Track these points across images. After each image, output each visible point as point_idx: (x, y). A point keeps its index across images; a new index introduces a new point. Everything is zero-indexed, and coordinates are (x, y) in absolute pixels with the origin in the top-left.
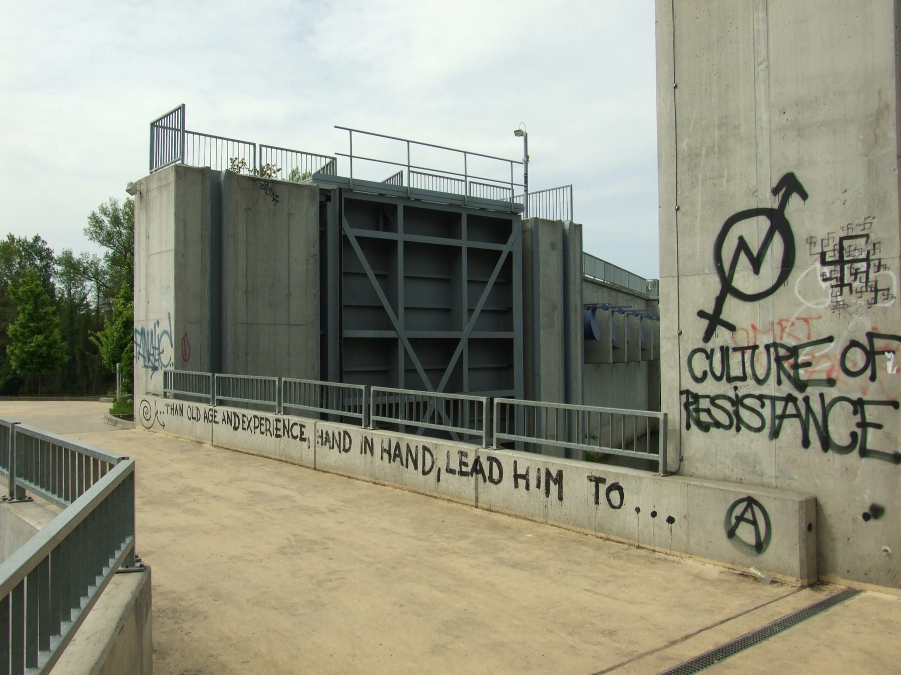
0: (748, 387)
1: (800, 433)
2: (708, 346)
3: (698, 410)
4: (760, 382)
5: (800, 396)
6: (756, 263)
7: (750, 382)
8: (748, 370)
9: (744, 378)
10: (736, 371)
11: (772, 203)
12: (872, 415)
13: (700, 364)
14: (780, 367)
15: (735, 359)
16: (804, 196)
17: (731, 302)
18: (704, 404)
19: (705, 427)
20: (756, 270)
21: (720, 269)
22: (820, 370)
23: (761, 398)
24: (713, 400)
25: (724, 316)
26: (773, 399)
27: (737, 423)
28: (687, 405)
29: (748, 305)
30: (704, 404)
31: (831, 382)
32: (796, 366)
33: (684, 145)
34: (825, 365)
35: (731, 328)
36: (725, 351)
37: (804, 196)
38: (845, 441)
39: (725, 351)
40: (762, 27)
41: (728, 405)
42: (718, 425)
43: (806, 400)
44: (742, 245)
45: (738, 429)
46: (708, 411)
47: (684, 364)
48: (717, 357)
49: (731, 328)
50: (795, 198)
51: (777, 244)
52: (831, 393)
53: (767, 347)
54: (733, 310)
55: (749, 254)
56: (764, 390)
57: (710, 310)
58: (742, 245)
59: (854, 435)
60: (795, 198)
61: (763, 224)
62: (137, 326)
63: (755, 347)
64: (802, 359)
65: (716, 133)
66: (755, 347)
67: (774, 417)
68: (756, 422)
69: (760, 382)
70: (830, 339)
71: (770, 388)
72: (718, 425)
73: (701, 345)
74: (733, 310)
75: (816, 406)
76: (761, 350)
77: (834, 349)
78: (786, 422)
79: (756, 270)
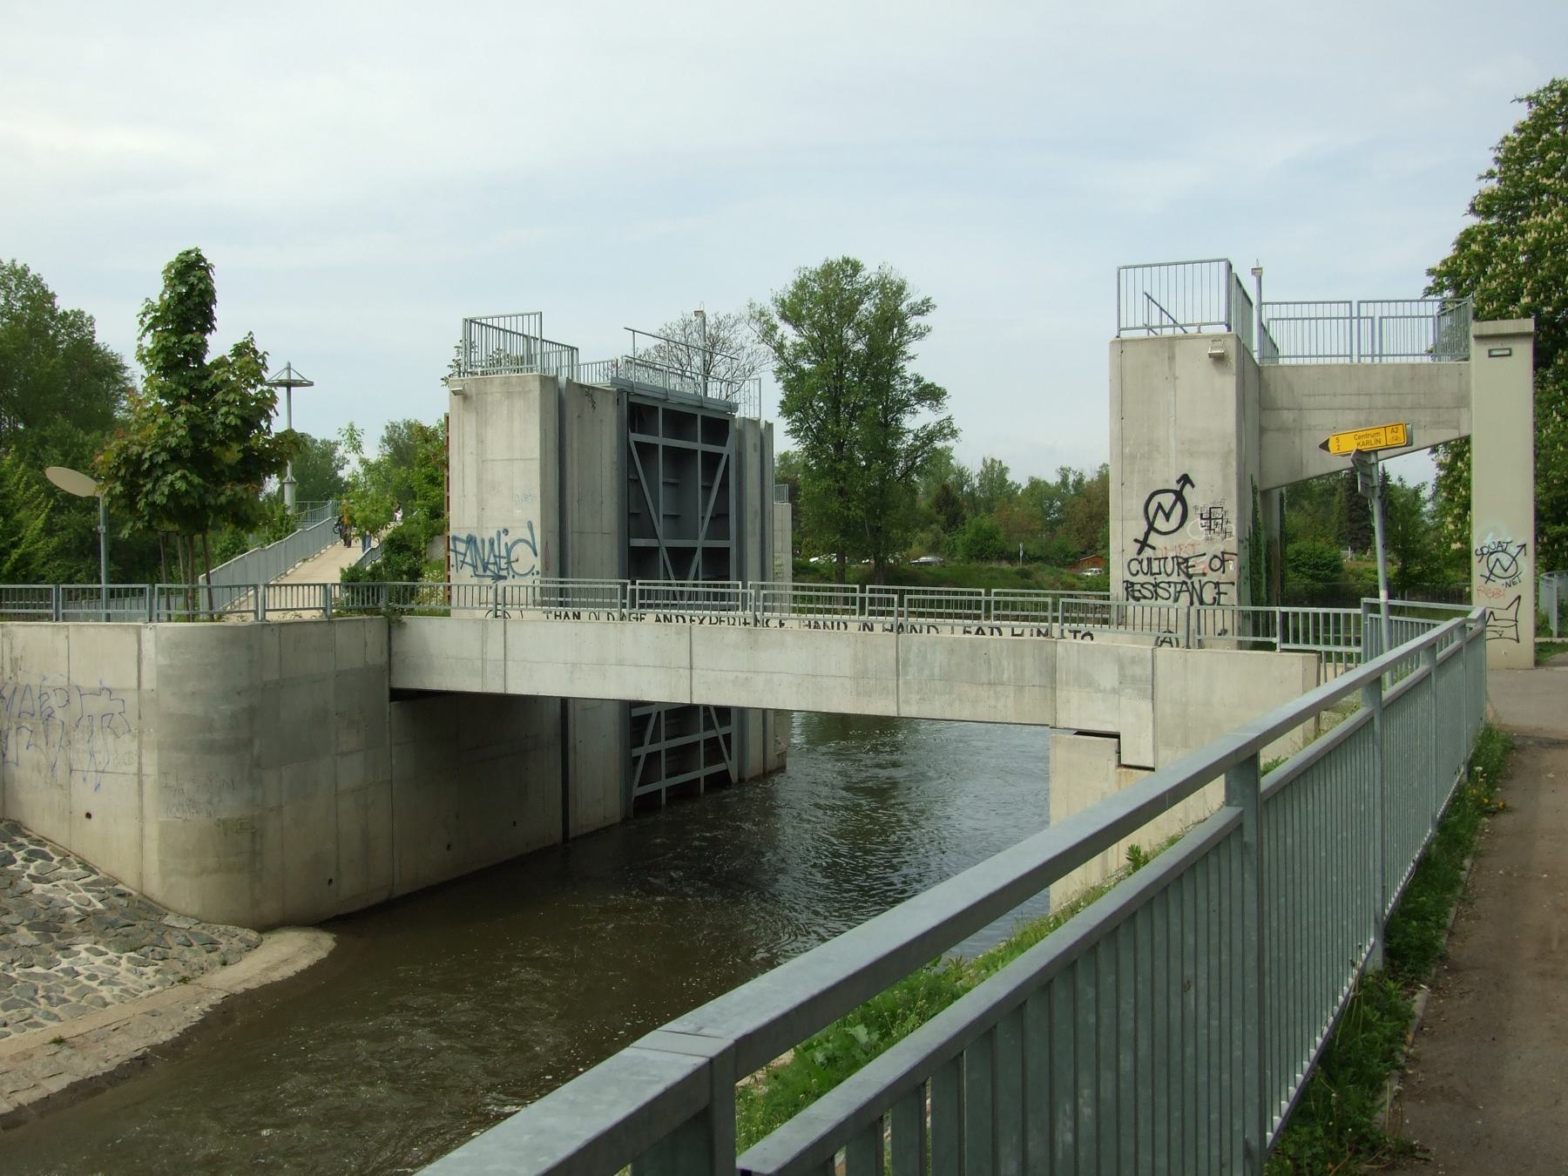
0: (1160, 578)
1: (1189, 599)
2: (1140, 557)
3: (1133, 591)
4: (1168, 575)
5: (1189, 582)
6: (1167, 516)
7: (1163, 575)
8: (1162, 569)
9: (1160, 573)
10: (1155, 570)
11: (1177, 487)
12: (1223, 588)
13: (1135, 566)
14: (1179, 568)
15: (1155, 564)
16: (1193, 486)
17: (1153, 535)
18: (1137, 587)
19: (1138, 599)
20: (1168, 520)
21: (1148, 518)
22: (1199, 569)
23: (1169, 583)
24: (1142, 585)
25: (1150, 542)
26: (1175, 583)
27: (1156, 596)
28: (1127, 589)
29: (1163, 536)
30: (1137, 587)
31: (1204, 574)
32: (1187, 567)
33: (1127, 450)
34: (1202, 566)
35: (1154, 548)
36: (1149, 560)
37: (1193, 486)
38: (1211, 601)
39: (1149, 560)
40: (1173, 398)
41: (1151, 588)
42: (1145, 597)
43: (1192, 583)
44: (1160, 506)
45: (1156, 599)
46: (1139, 591)
47: (1125, 566)
48: (1145, 563)
49: (1154, 548)
50: (1188, 486)
51: (1179, 508)
52: (1205, 579)
53: (1173, 558)
54: (1154, 539)
55: (1164, 511)
56: (1170, 579)
57: (1141, 539)
58: (1160, 506)
59: (1215, 598)
60: (1188, 486)
61: (1172, 497)
62: (461, 518)
63: (1166, 558)
64: (1190, 564)
65: (1146, 448)
66: (1166, 558)
67: (1176, 592)
68: (1167, 595)
69: (1168, 575)
70: (1204, 554)
71: (1174, 578)
72: (1145, 597)
73: (1136, 557)
74: (1154, 539)
75: (1197, 586)
76: (1170, 559)
77: (1206, 559)
78: (1182, 594)
79: (1168, 520)
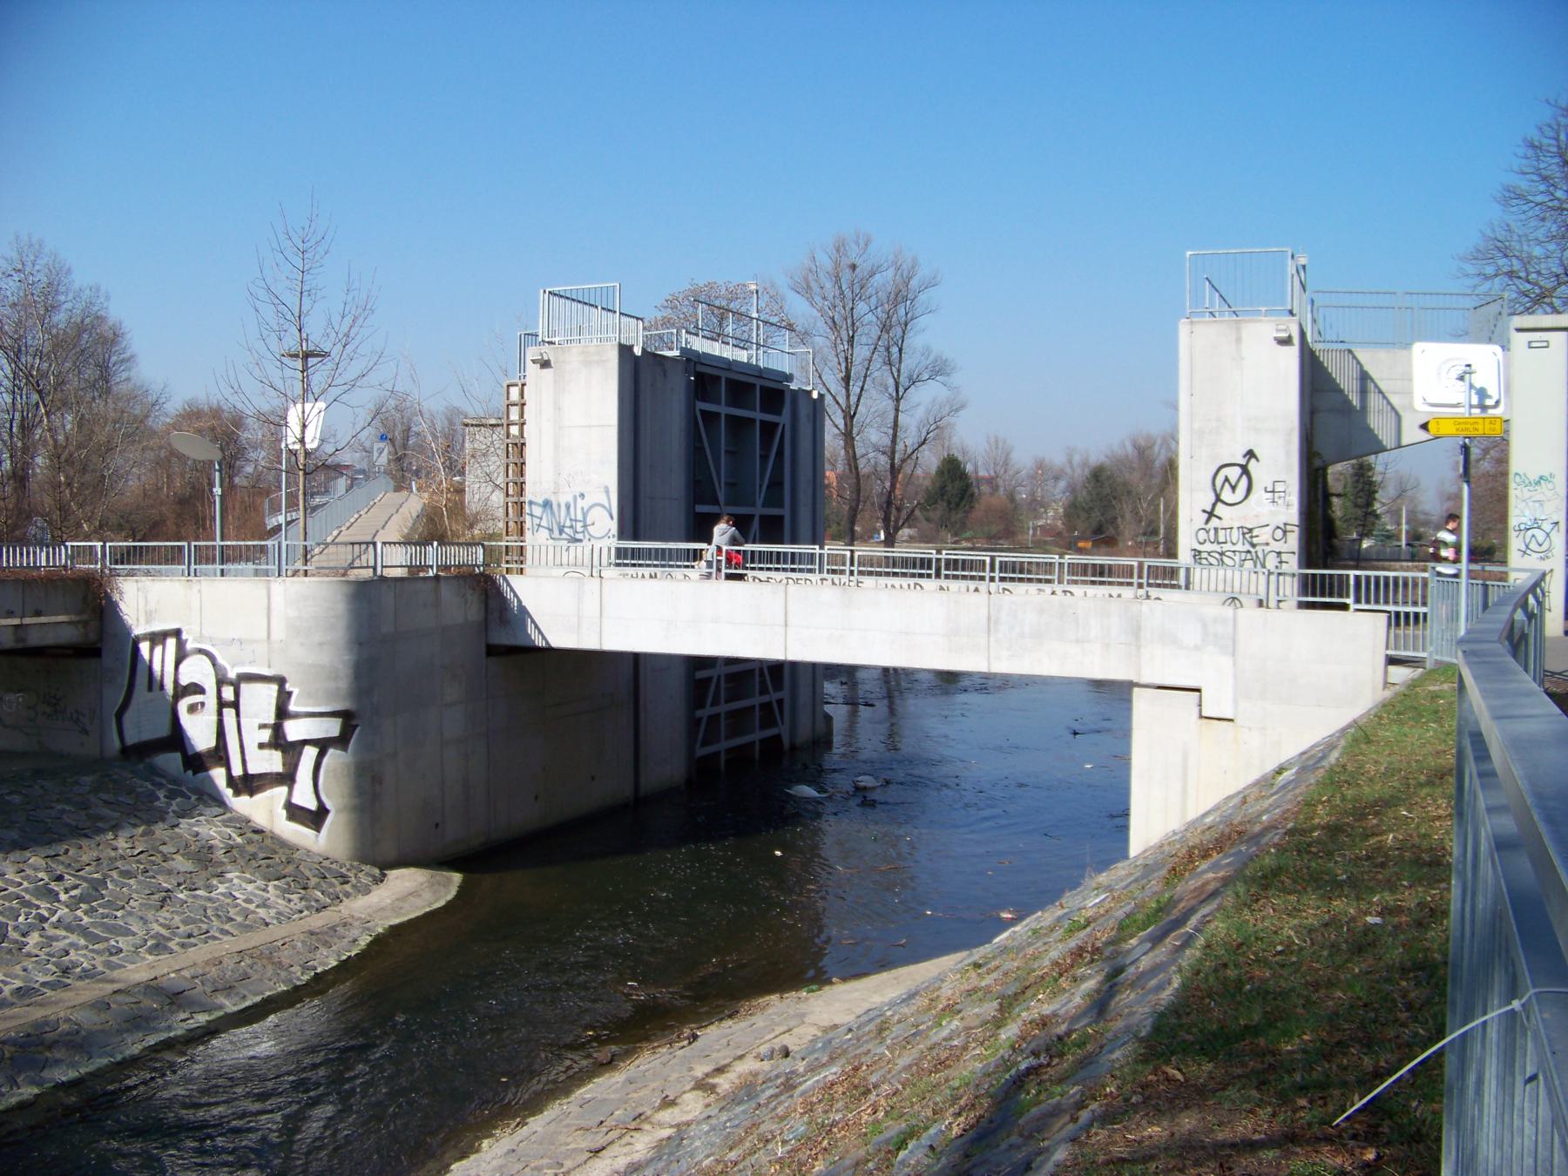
2: (1207, 527)
6: (1233, 488)
10: (1221, 539)
11: (1243, 462)
12: (1284, 557)
13: (1202, 535)
14: (1244, 537)
15: (1221, 533)
16: (1258, 460)
18: (1204, 555)
21: (1215, 490)
23: (1234, 552)
24: (1209, 553)
28: (1195, 556)
30: (1204, 555)
31: (1267, 544)
32: (1252, 537)
35: (1220, 518)
37: (1258, 460)
41: (1217, 556)
43: (1256, 552)
44: (1227, 479)
46: (1206, 559)
48: (1212, 532)
49: (1220, 518)
50: (1253, 460)
52: (1267, 549)
54: (1220, 510)
58: (1227, 479)
61: (1238, 470)
66: (1231, 528)
69: (1234, 544)
71: (1239, 547)
73: (1204, 526)
74: (1220, 510)
